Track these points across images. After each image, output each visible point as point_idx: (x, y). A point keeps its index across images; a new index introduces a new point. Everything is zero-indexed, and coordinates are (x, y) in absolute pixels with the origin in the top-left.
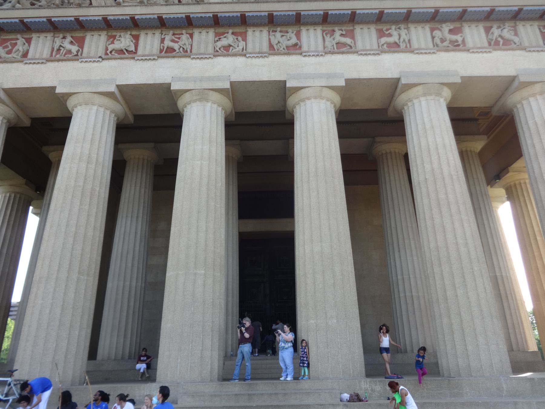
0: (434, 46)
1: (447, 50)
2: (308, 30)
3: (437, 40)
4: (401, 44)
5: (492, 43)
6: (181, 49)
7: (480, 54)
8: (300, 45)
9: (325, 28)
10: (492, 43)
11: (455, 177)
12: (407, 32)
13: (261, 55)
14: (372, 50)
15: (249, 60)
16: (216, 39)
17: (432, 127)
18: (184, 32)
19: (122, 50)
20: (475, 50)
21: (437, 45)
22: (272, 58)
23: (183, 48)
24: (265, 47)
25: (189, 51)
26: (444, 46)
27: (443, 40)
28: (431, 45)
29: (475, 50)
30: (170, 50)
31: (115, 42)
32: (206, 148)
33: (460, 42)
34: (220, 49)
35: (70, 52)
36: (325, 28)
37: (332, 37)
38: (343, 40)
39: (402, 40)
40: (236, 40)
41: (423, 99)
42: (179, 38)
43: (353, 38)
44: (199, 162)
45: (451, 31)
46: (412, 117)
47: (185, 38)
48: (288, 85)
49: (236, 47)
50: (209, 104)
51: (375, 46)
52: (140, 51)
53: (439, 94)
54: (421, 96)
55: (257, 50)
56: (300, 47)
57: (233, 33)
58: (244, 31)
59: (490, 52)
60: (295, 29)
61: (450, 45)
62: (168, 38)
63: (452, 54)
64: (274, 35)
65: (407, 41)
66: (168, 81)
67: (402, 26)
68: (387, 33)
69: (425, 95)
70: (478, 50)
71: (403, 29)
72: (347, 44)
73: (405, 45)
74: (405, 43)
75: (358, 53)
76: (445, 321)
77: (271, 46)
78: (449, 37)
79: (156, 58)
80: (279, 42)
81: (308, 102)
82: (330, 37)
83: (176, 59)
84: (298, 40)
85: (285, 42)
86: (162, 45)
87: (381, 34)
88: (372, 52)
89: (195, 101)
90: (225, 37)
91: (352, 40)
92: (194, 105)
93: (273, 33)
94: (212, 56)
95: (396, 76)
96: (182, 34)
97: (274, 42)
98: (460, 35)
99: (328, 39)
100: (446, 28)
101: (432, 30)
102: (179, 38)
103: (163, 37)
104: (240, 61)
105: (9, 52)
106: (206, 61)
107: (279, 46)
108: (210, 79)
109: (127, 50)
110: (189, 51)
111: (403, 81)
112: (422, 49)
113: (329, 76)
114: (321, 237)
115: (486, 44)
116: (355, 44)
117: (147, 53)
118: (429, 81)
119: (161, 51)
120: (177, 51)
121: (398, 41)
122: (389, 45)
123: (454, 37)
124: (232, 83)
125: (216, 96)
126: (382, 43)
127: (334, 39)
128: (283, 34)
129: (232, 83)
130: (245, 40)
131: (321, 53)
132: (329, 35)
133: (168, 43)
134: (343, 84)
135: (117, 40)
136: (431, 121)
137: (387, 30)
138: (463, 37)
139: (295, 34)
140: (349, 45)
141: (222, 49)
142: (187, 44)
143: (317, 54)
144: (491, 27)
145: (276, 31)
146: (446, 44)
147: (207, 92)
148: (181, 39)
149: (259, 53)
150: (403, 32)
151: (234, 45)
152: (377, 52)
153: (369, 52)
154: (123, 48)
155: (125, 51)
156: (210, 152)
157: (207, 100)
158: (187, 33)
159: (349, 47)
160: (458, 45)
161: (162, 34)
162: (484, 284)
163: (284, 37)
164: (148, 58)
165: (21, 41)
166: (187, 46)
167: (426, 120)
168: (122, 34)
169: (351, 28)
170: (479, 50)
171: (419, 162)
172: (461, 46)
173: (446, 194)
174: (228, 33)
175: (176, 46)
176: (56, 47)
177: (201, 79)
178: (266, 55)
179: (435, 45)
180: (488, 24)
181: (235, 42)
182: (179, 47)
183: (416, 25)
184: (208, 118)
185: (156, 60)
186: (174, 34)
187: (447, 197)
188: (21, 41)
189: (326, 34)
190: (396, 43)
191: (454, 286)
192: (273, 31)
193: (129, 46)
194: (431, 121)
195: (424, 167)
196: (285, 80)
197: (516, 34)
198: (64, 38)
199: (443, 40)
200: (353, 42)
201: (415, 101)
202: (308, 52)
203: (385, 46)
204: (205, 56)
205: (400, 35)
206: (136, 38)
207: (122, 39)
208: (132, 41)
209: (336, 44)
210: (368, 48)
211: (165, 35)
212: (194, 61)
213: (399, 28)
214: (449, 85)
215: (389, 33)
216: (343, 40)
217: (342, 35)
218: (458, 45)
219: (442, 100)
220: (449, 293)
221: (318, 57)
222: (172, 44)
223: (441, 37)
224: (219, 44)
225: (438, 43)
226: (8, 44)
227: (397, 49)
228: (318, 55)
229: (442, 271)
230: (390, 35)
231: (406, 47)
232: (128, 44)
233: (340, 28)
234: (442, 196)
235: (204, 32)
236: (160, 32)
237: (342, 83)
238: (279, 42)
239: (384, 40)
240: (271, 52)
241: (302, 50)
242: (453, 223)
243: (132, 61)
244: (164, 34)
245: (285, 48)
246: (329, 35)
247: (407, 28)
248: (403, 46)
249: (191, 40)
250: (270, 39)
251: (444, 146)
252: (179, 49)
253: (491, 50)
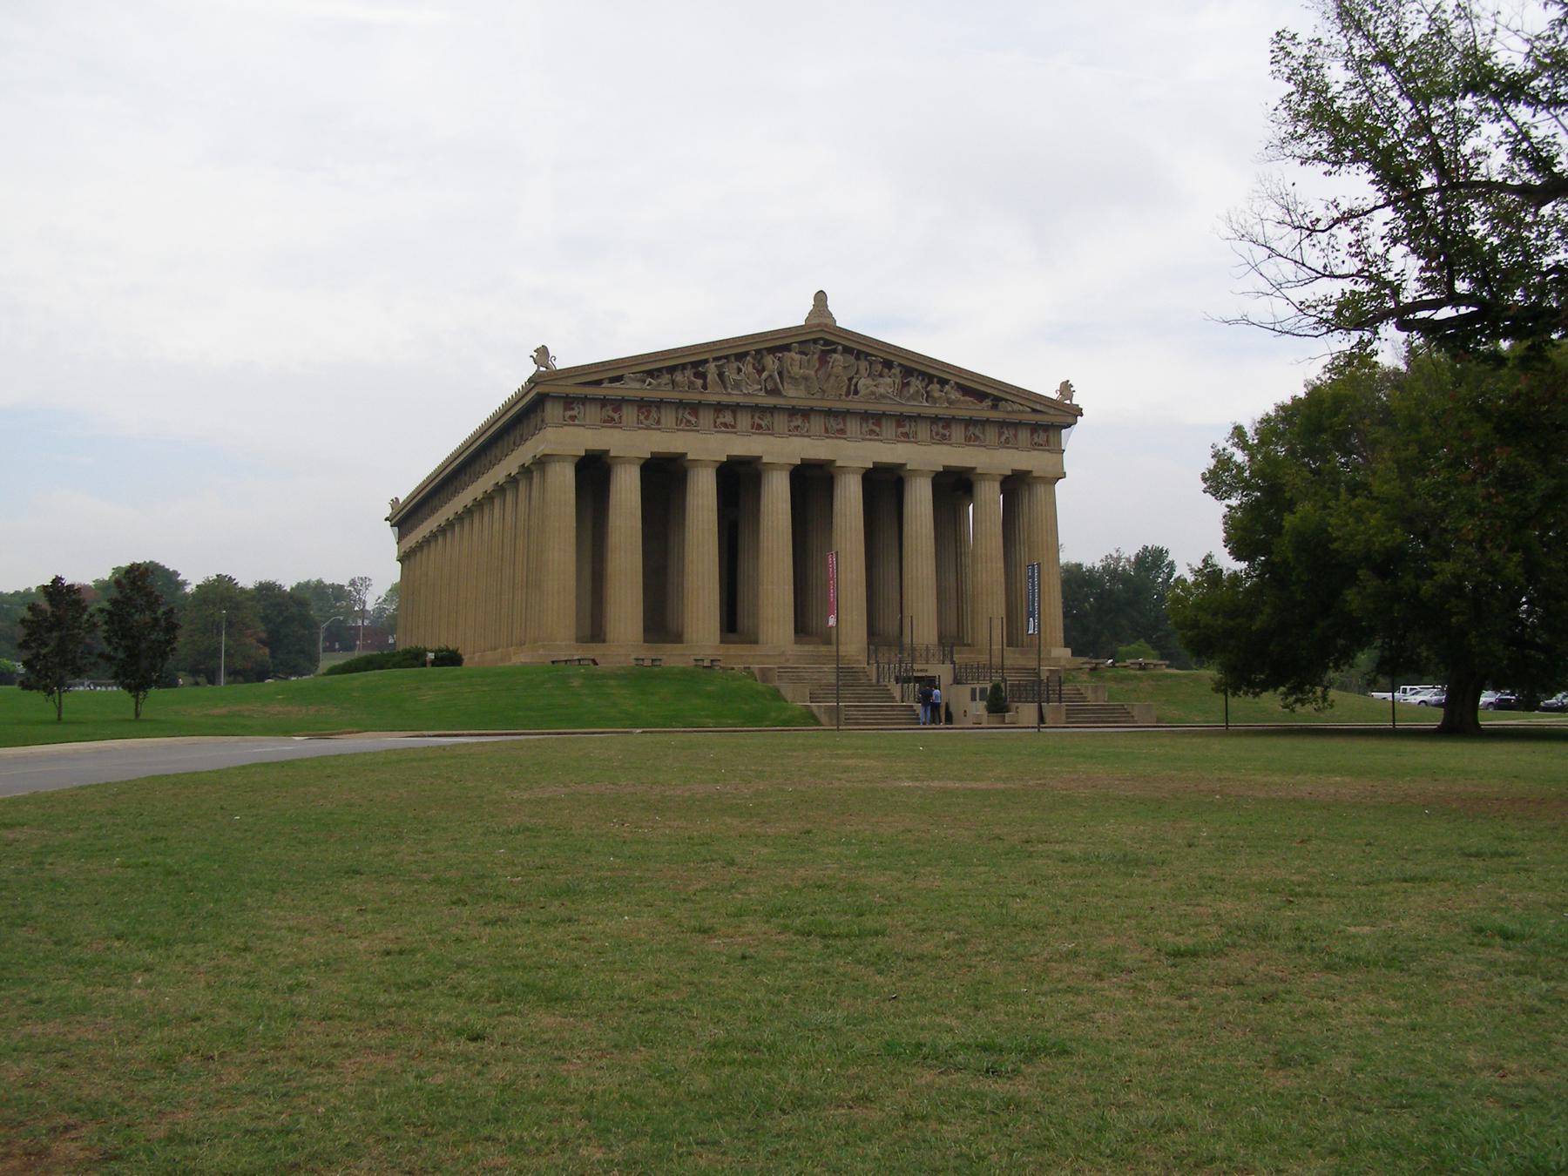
1: (940, 443)
3: (934, 433)
17: (921, 501)
27: (937, 434)
30: (759, 427)
31: (721, 416)
35: (689, 421)
43: (880, 427)
45: (943, 427)
47: (769, 415)
52: (739, 427)
77: (827, 430)
78: (941, 431)
85: (836, 427)
87: (899, 425)
99: (864, 425)
105: (647, 418)
133: (757, 420)
146: (938, 438)
150: (913, 424)
165: (654, 410)
170: (960, 445)
175: (763, 424)
176: (680, 417)
179: (932, 438)
188: (654, 410)
197: (983, 433)
198: (685, 408)
199: (937, 434)
216: (874, 428)
222: (760, 422)
226: (644, 410)
230: (904, 426)
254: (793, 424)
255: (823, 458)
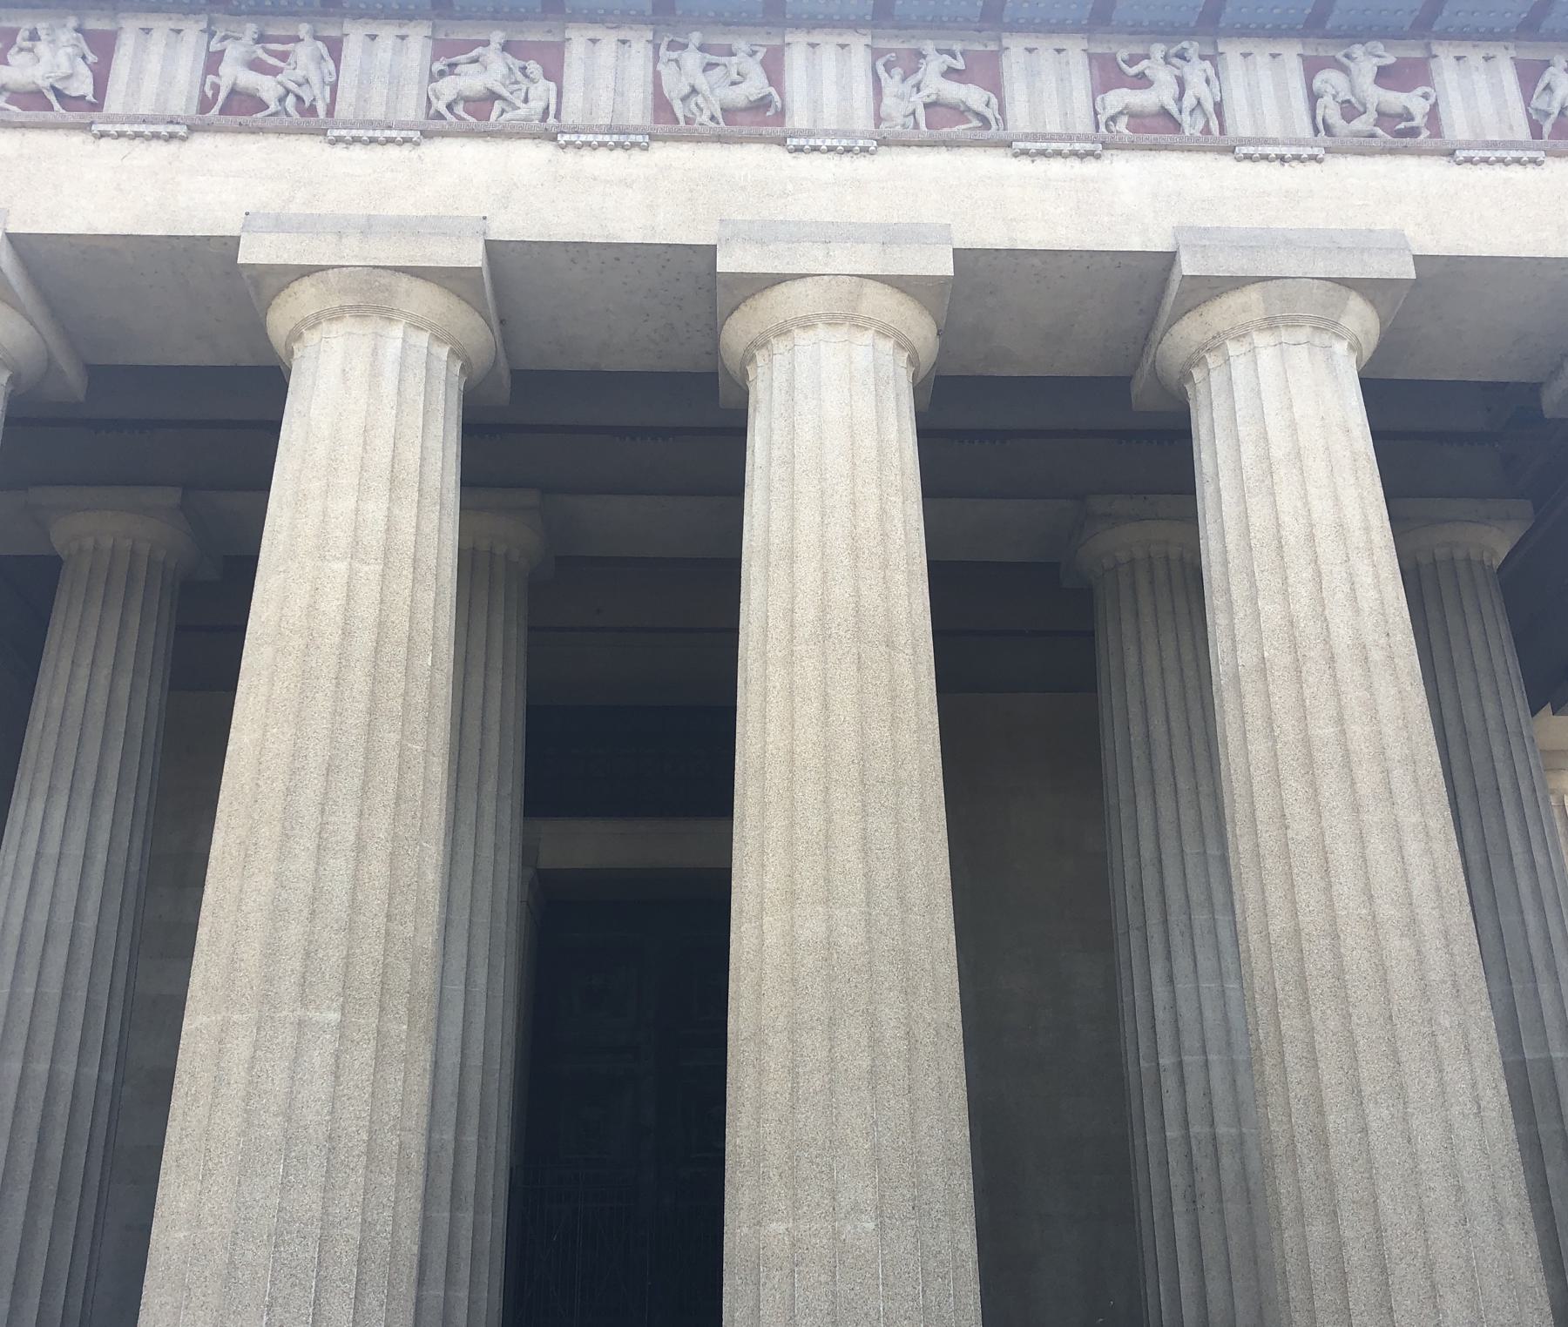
0: (1317, 131)
1: (1363, 148)
2: (813, 45)
3: (1330, 110)
4: (1186, 119)
5: (1547, 127)
6: (291, 100)
7: (1499, 170)
8: (779, 105)
9: (882, 44)
10: (1547, 127)
11: (1376, 655)
12: (1211, 72)
13: (620, 137)
14: (1069, 138)
15: (569, 157)
16: (437, 66)
18: (304, 29)
19: (38, 93)
20: (1477, 154)
21: (1328, 130)
22: (664, 154)
23: (299, 98)
24: (637, 111)
25: (321, 108)
26: (1357, 134)
28: (1304, 129)
29: (1477, 154)
32: (375, 510)
33: (1419, 121)
34: (449, 107)
36: (882, 44)
37: (912, 81)
38: (955, 91)
39: (1189, 101)
40: (519, 76)
41: (1262, 340)
42: (284, 57)
43: (995, 85)
44: (341, 567)
45: (1384, 76)
46: (1220, 413)
48: (724, 265)
49: (519, 103)
50: (397, 331)
51: (1083, 125)
52: (115, 102)
53: (1327, 325)
54: (1260, 330)
55: (604, 120)
56: (781, 114)
57: (506, 47)
58: (557, 39)
59: (1535, 162)
60: (764, 41)
61: (1379, 131)
62: (234, 53)
63: (1380, 165)
64: (677, 61)
65: (1209, 106)
66: (228, 226)
67: (1193, 48)
68: (1133, 71)
69: (1271, 324)
70: (1487, 154)
71: (1195, 59)
72: (969, 109)
73: (1200, 125)
74: (1204, 114)
75: (1010, 146)
76: (1317, 1231)
77: (661, 106)
79: (181, 130)
80: (694, 91)
81: (803, 338)
82: (904, 80)
83: (272, 140)
84: (770, 85)
85: (719, 92)
86: (210, 78)
87: (1107, 75)
88: (1065, 147)
89: (336, 315)
90: (475, 61)
91: (992, 95)
92: (337, 329)
93: (674, 55)
94: (415, 135)
95: (1160, 244)
96: (298, 40)
97: (674, 87)
98: (1420, 91)
99: (892, 85)
100: (1366, 61)
101: (1311, 68)
102: (284, 57)
103: (215, 46)
104: (529, 157)
106: (393, 152)
107: (693, 106)
108: (402, 227)
109: (59, 94)
110: (321, 108)
111: (1188, 266)
112: (1266, 142)
113: (890, 236)
114: (827, 880)
115: (1523, 132)
116: (1002, 110)
117: (145, 108)
118: (1290, 267)
119: (205, 105)
120: (273, 107)
121: (1173, 109)
122: (1137, 119)
123: (1395, 100)
124: (492, 248)
125: (426, 299)
126: (1111, 112)
127: (918, 87)
128: (714, 59)
129: (492, 248)
130: (554, 73)
131: (861, 143)
132: (897, 72)
133: (233, 73)
134: (946, 268)
135: (21, 50)
136: (1293, 426)
137: (1132, 61)
138: (1432, 100)
139: (763, 63)
140: (978, 115)
141: (459, 109)
142: (315, 79)
143: (845, 142)
144: (1547, 64)
145: (685, 46)
146: (1362, 124)
147: (386, 279)
148: (291, 59)
149: (610, 130)
150: (1196, 72)
151: (512, 93)
152: (1089, 146)
153: (1054, 146)
154: (44, 84)
155: (52, 97)
156: (390, 527)
157: (387, 314)
158: (316, 38)
159: (976, 123)
160: (1413, 132)
161: (212, 35)
162: (1474, 1086)
163: (718, 71)
164: (147, 129)
166: (317, 92)
167: (1275, 425)
168: (42, 27)
169: (992, 47)
171: (1239, 591)
172: (1425, 133)
173: (1340, 720)
174: (486, 43)
175: (267, 88)
177: (368, 227)
178: (639, 138)
180: (1532, 54)
181: (516, 82)
182: (281, 91)
183: (1248, 45)
184: (388, 386)
185: (183, 139)
186: (261, 39)
187: (1343, 732)
189: (888, 67)
190: (1164, 113)
191: (1356, 1090)
192: (672, 46)
193: (69, 77)
194: (1293, 426)
195: (1257, 614)
196: (712, 242)
199: (1350, 111)
200: (994, 101)
201: (1233, 348)
202: (810, 134)
203: (1122, 125)
204: (388, 133)
205: (1181, 83)
206: (102, 48)
207: (42, 48)
208: (84, 58)
209: (926, 106)
210: (1053, 127)
211: (225, 38)
212: (339, 150)
213: (1181, 56)
214: (1369, 288)
215: (1141, 76)
216: (955, 91)
217: (950, 73)
218: (1413, 132)
219: (1341, 348)
220: (1336, 1121)
221: (846, 158)
222: (249, 79)
223: (1345, 95)
224: (448, 88)
225: (1330, 121)
227: (1167, 138)
228: (848, 150)
229: (1311, 1030)
230: (1143, 81)
231: (1207, 130)
232: (65, 69)
233: (944, 45)
234: (1323, 730)
235: (387, 33)
236: (204, 25)
237: (944, 266)
238: (694, 91)
239: (1117, 99)
240: (661, 128)
241: (788, 125)
242: (1361, 839)
243: (77, 140)
244: (219, 35)
245: (719, 115)
246: (897, 72)
247: (1214, 59)
248: (1192, 126)
249: (331, 66)
250: (657, 77)
251: (1341, 527)
252: (281, 100)
253: (1540, 155)
254: (470, 80)
255: (631, 233)
